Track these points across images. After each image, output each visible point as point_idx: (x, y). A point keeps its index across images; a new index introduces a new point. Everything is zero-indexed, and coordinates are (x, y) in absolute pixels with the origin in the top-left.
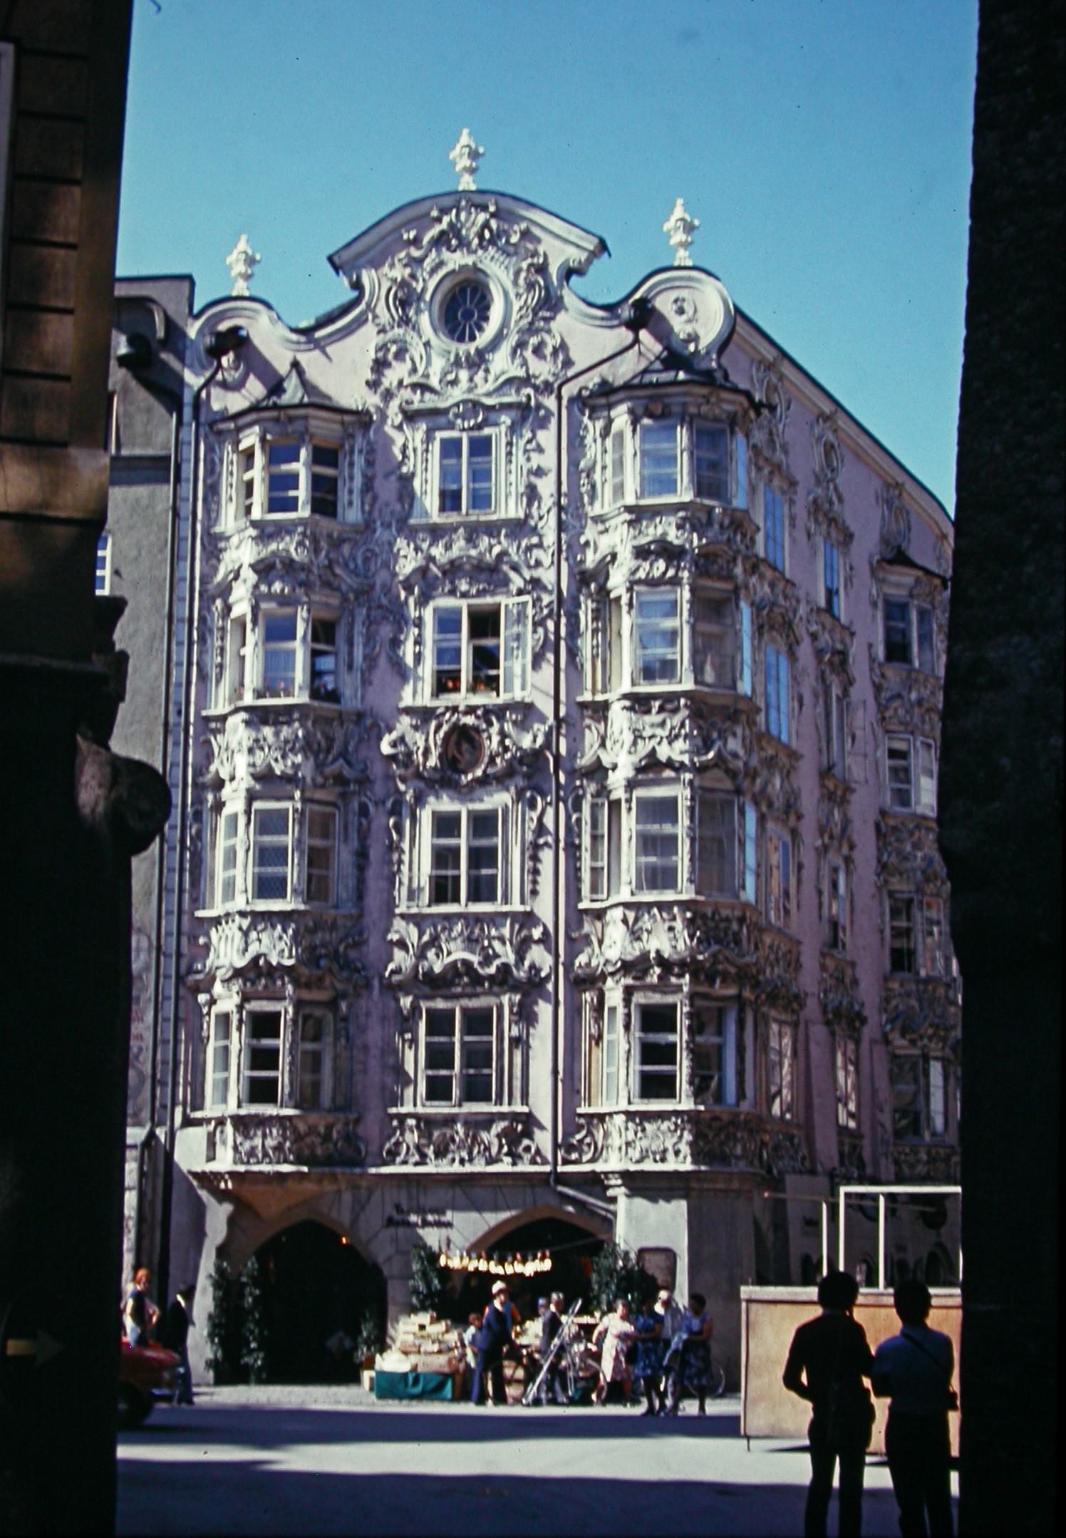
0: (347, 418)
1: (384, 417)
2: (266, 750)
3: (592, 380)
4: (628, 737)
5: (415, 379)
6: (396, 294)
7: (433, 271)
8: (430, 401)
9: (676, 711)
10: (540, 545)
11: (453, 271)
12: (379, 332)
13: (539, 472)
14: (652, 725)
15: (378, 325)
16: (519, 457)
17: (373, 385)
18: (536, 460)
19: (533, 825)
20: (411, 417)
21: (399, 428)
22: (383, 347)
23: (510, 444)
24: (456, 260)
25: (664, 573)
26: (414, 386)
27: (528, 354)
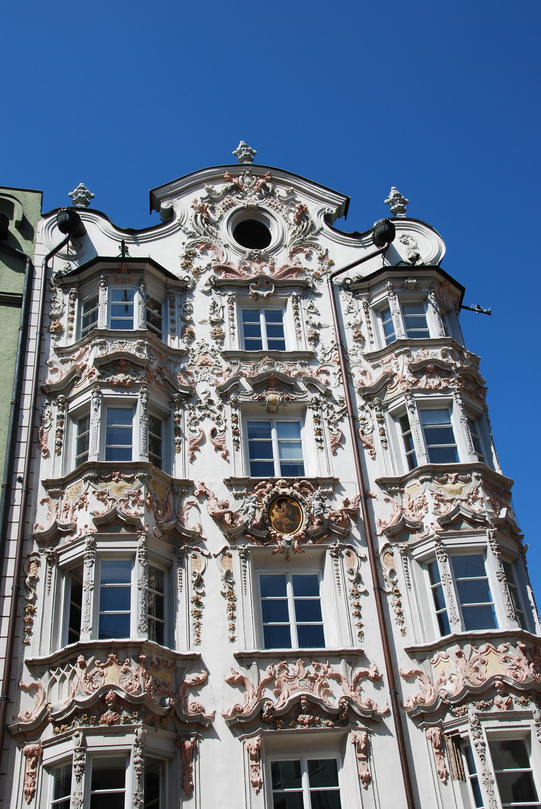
0: (170, 281)
1: (194, 285)
4: (431, 501)
5: (218, 264)
6: (202, 217)
7: (226, 208)
8: (231, 277)
9: (469, 481)
11: (242, 208)
12: (190, 237)
13: (320, 326)
14: (452, 492)
15: (187, 234)
16: (304, 315)
17: (186, 267)
18: (316, 320)
19: (353, 578)
20: (218, 286)
23: (296, 308)
25: (440, 384)
27: (301, 256)
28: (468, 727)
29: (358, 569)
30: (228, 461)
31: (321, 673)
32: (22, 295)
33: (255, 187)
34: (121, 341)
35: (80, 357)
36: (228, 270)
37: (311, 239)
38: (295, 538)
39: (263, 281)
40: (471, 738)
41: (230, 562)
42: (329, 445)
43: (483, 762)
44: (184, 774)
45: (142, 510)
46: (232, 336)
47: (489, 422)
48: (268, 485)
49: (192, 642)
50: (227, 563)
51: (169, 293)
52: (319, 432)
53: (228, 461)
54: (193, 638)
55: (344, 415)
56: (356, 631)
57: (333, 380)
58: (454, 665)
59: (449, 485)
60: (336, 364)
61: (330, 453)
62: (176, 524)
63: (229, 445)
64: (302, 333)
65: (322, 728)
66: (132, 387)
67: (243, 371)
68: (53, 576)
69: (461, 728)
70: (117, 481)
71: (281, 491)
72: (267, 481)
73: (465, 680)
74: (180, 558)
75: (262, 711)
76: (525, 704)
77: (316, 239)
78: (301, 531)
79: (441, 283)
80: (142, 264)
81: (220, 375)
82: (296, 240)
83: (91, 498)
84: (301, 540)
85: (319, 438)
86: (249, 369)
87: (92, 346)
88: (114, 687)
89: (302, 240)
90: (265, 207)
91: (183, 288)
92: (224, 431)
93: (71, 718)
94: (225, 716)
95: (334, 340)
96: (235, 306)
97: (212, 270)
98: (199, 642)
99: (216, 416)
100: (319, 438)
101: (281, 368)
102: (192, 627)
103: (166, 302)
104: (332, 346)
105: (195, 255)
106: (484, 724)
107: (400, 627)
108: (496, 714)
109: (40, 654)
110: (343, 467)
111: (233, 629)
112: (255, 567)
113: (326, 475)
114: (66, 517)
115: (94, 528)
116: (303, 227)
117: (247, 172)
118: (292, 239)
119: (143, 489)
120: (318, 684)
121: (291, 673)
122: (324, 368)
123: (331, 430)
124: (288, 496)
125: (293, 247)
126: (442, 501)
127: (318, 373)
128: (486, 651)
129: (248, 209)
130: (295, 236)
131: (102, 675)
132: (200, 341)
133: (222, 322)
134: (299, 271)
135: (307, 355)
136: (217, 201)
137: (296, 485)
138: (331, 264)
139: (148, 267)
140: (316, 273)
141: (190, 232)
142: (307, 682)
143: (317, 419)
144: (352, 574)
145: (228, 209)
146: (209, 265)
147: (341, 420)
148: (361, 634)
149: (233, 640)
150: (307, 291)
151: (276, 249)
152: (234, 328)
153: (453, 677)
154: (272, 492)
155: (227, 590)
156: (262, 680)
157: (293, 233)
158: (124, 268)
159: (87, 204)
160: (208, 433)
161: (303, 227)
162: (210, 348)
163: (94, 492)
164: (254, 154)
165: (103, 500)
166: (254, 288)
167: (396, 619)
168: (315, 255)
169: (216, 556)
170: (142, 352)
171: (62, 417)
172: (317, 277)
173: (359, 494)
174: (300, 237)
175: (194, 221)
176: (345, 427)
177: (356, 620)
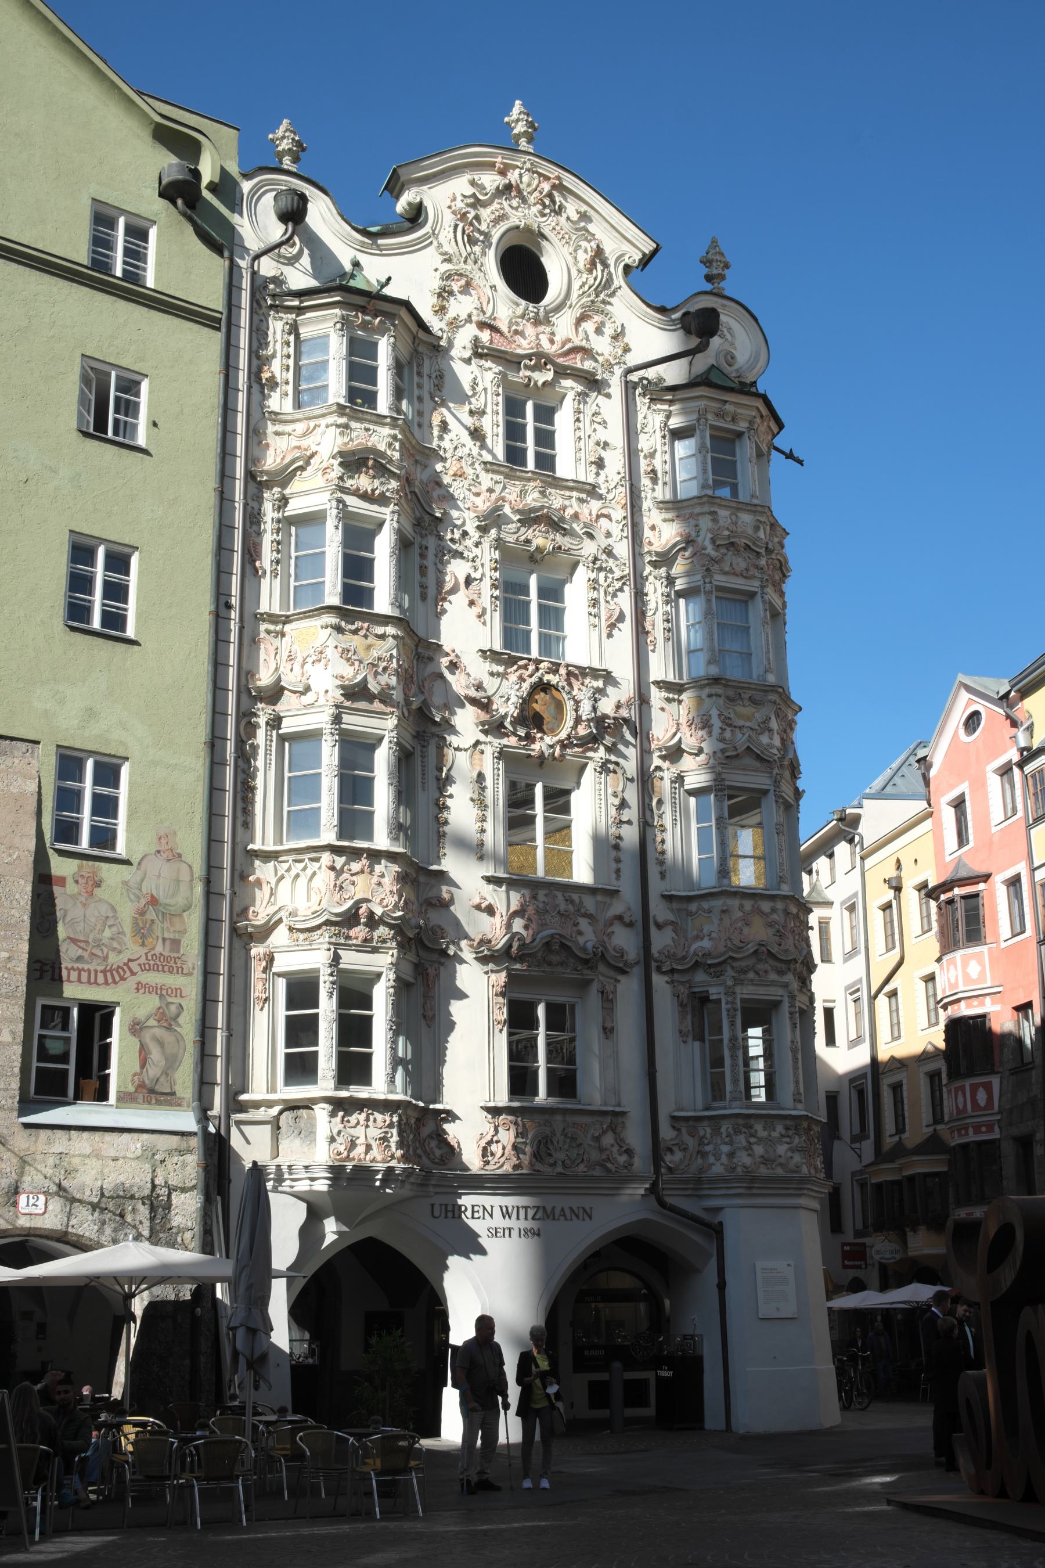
1: (451, 343)
2: (357, 663)
3: (651, 373)
5: (482, 318)
7: (497, 221)
8: (500, 344)
10: (608, 517)
11: (518, 227)
12: (445, 260)
18: (602, 435)
19: (617, 802)
20: (479, 352)
21: (468, 361)
22: (448, 277)
23: (578, 412)
24: (516, 218)
26: (482, 325)
28: (721, 989)
29: (623, 791)
30: (484, 624)
31: (571, 908)
32: (221, 313)
33: (536, 194)
34: (367, 426)
35: (304, 435)
36: (494, 329)
37: (604, 302)
38: (558, 742)
39: (541, 360)
40: (723, 1002)
41: (481, 760)
42: (604, 625)
44: (425, 1003)
45: (393, 681)
46: (495, 438)
47: (785, 624)
48: (531, 668)
50: (476, 762)
51: (416, 350)
52: (595, 602)
53: (484, 624)
55: (624, 584)
57: (616, 529)
58: (716, 922)
59: (739, 709)
60: (619, 507)
61: (604, 635)
62: (424, 702)
63: (486, 601)
64: (583, 451)
66: (382, 500)
67: (507, 496)
68: (274, 744)
69: (712, 990)
70: (366, 636)
71: (547, 678)
72: (530, 660)
73: (728, 942)
74: (423, 746)
75: (511, 946)
76: (781, 973)
77: (610, 303)
78: (563, 735)
79: (762, 416)
80: (396, 307)
81: (478, 495)
82: (585, 300)
83: (330, 652)
84: (564, 745)
85: (593, 611)
86: (515, 495)
87: (327, 426)
88: (368, 901)
89: (593, 302)
90: (546, 231)
91: (434, 346)
92: (481, 580)
93: (318, 927)
95: (622, 471)
96: (500, 390)
97: (474, 325)
99: (471, 556)
100: (593, 611)
101: (556, 500)
103: (410, 363)
104: (617, 478)
105: (451, 293)
106: (738, 990)
108: (752, 980)
109: (263, 844)
110: (618, 656)
112: (506, 771)
113: (596, 665)
114: (292, 670)
115: (337, 695)
116: (595, 279)
117: (528, 165)
118: (580, 296)
119: (394, 652)
122: (604, 511)
123: (607, 602)
124: (553, 686)
125: (580, 311)
126: (730, 725)
127: (598, 517)
129: (528, 230)
130: (584, 293)
131: (353, 883)
132: (455, 438)
133: (484, 413)
134: (587, 352)
135: (588, 487)
136: (485, 205)
137: (563, 671)
138: (627, 350)
139: (403, 313)
140: (607, 361)
141: (446, 254)
143: (594, 585)
144: (616, 796)
145: (498, 223)
146: (470, 316)
147: (621, 590)
148: (618, 871)
150: (593, 384)
151: (558, 309)
152: (498, 426)
153: (714, 935)
154: (534, 679)
155: (476, 797)
156: (511, 911)
157: (581, 287)
158: (370, 307)
159: (296, 160)
160: (462, 581)
161: (595, 279)
162: (466, 451)
163: (336, 647)
164: (535, 129)
165: (348, 660)
166: (527, 367)
168: (608, 330)
169: (466, 750)
170: (394, 449)
171: (279, 521)
172: (609, 367)
173: (632, 695)
174: (589, 296)
175: (452, 235)
176: (625, 601)
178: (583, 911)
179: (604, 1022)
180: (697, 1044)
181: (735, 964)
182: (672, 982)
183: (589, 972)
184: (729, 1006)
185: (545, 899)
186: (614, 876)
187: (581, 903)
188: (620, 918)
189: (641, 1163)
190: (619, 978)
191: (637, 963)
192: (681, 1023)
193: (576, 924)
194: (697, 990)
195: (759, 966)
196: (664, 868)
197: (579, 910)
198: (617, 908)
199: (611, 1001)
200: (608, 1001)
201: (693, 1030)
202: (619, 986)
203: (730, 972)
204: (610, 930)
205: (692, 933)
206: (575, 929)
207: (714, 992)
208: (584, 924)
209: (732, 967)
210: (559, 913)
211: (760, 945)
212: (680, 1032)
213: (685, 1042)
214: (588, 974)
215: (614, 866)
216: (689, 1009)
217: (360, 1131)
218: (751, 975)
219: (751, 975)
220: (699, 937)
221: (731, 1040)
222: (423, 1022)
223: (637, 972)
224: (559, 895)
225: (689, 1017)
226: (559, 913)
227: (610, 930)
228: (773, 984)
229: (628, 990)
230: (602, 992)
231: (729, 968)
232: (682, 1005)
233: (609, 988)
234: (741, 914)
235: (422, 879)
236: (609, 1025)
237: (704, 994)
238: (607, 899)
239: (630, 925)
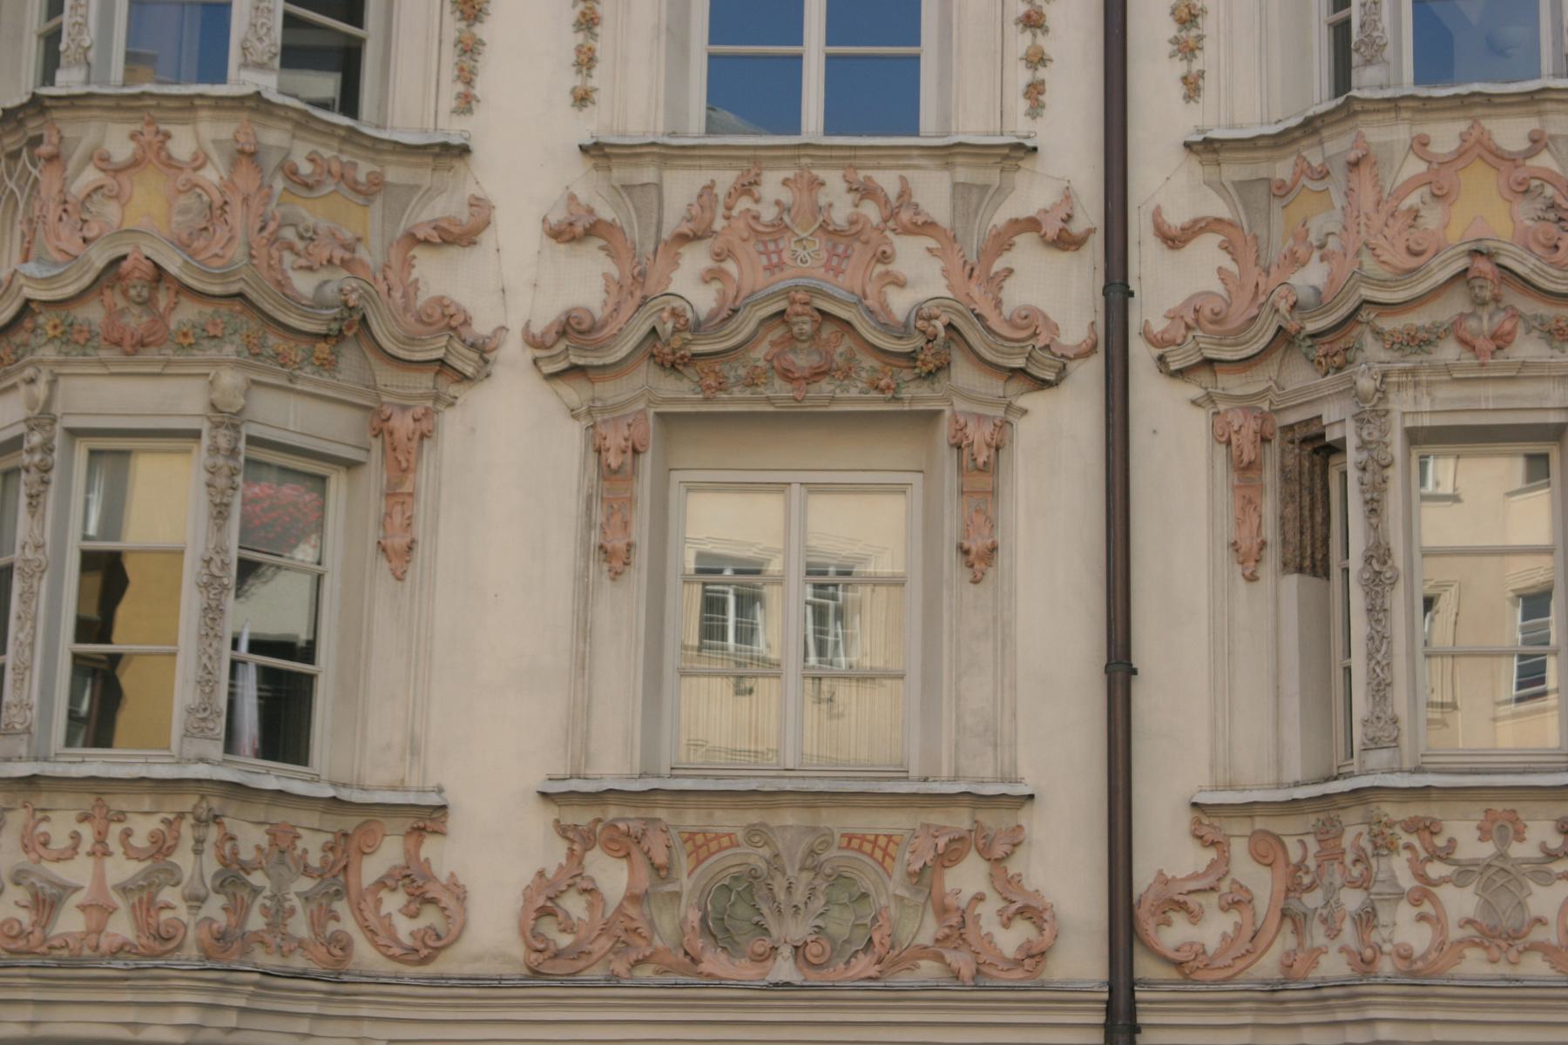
43: (1374, 521)
49: (448, 101)
54: (451, 90)
56: (1023, 76)
65: (854, 393)
94: (532, 341)
98: (466, 104)
102: (450, 55)
107: (1180, 67)
108: (1448, 368)
111: (586, 61)
120: (859, 252)
121: (768, 214)
128: (1461, 154)
142: (819, 245)
148: (1035, 91)
149: (582, 99)
153: (1332, 244)
156: (666, 234)
167: (1175, 41)
177: (1022, 42)
178: (905, 216)
179: (966, 533)
180: (1293, 579)
181: (1388, 324)
182: (1210, 399)
183: (923, 390)
184: (1364, 455)
185: (786, 196)
186: (1023, 105)
187: (905, 193)
188: (1033, 224)
189: (1081, 960)
190: (1024, 401)
191: (1093, 349)
192: (1239, 523)
193: (885, 258)
194: (1292, 418)
195: (1472, 324)
196: (1196, 66)
197: (894, 215)
198: (1031, 194)
199: (988, 469)
200: (982, 471)
201: (1285, 542)
202: (1023, 426)
203: (1373, 352)
204: (998, 265)
205: (1279, 245)
206: (880, 268)
207: (1337, 419)
208: (911, 255)
209: (1378, 334)
210: (823, 227)
211: (1476, 253)
212: (1234, 546)
213: (1252, 578)
214: (919, 396)
215: (1023, 76)
216: (1270, 476)
217: (79, 871)
218: (1449, 352)
219: (1449, 352)
220: (1296, 261)
221: (1368, 560)
222: (384, 564)
223: (1088, 376)
224: (834, 179)
225: (1269, 506)
226: (823, 227)
227: (998, 265)
228: (1522, 373)
229: (1056, 435)
230: (959, 447)
231: (1369, 339)
232: (1245, 470)
233: (979, 434)
234: (1422, 167)
235: (395, 173)
236: (977, 544)
237: (1314, 430)
238: (993, 176)
239: (1065, 242)
